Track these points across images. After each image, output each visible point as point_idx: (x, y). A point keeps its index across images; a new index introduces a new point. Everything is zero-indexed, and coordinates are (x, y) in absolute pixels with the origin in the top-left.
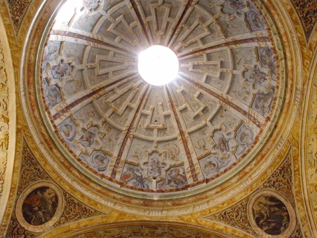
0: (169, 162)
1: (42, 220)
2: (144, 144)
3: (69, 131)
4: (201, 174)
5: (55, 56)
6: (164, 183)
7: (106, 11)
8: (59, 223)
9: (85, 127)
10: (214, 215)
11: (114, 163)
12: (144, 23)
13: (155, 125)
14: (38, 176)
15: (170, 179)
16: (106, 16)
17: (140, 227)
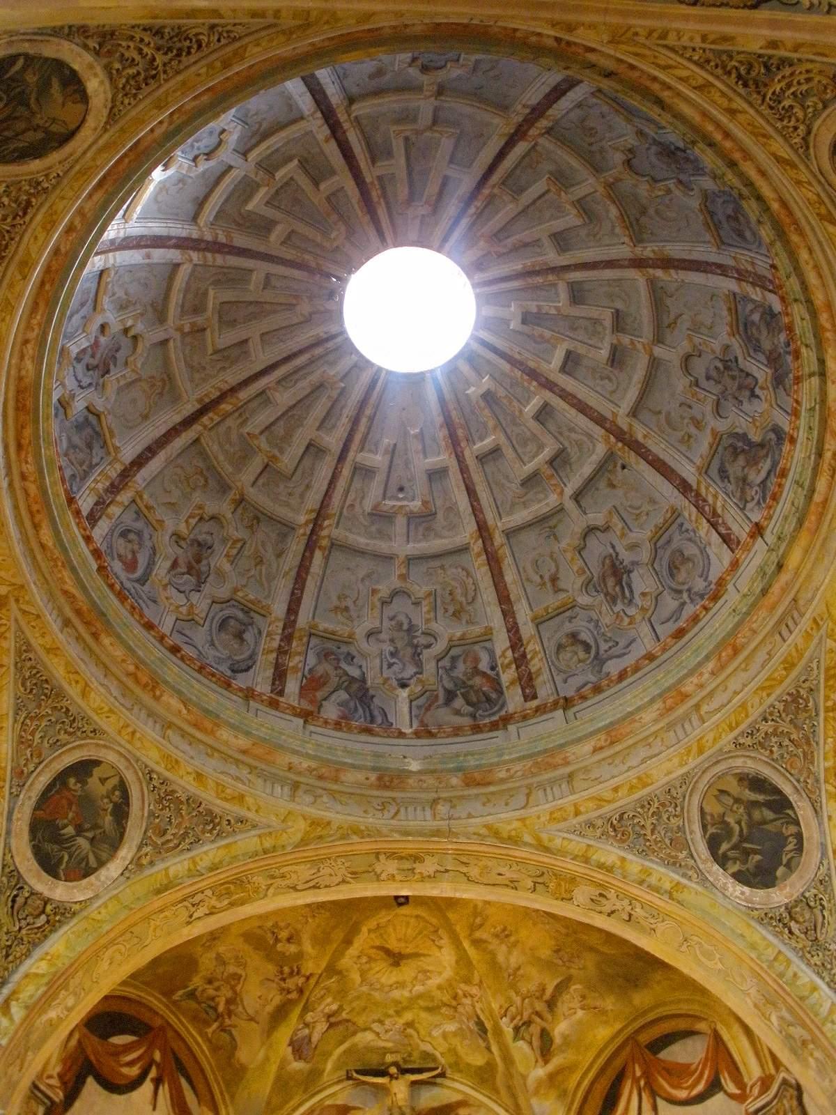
0: (447, 630)
1: (87, 863)
2: (365, 566)
3: (134, 552)
4: (545, 676)
5: (84, 317)
6: (433, 703)
7: (245, 154)
8: (137, 864)
9: (183, 529)
10: (591, 825)
11: (278, 638)
12: (368, 180)
13: (399, 504)
14: (66, 732)
15: (449, 685)
16: (242, 169)
17: (373, 857)
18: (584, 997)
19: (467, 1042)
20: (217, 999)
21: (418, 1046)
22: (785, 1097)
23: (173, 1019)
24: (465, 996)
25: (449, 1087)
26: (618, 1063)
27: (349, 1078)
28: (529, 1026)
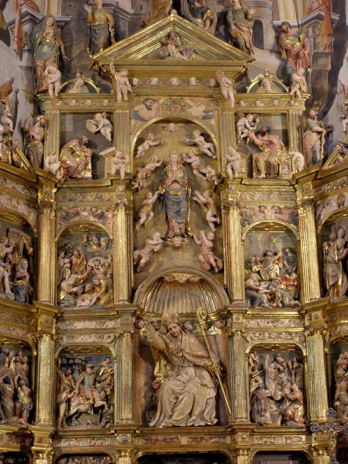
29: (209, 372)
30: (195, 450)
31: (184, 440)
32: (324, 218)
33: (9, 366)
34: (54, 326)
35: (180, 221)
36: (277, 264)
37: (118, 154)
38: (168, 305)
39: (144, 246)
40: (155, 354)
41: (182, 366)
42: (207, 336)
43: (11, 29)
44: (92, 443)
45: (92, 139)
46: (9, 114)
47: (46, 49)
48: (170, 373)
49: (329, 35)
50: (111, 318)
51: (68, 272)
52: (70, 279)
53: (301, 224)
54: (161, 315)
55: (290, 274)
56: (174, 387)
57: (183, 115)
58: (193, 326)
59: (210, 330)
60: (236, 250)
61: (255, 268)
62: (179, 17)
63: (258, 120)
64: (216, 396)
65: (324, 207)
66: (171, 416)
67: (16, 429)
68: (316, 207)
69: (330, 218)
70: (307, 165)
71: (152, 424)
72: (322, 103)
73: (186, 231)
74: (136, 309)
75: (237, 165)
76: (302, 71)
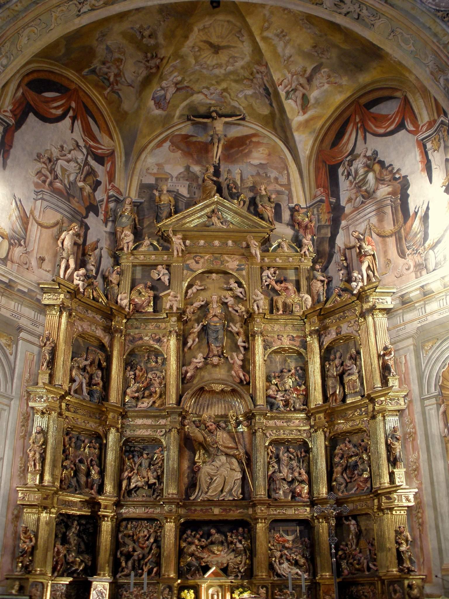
18: (329, 76)
19: (258, 101)
20: (109, 74)
21: (230, 102)
22: (441, 131)
23: (82, 85)
24: (258, 73)
25: (247, 126)
26: (346, 115)
27: (189, 119)
28: (295, 92)
29: (237, 459)
30: (225, 518)
31: (216, 511)
32: (326, 344)
33: (84, 450)
34: (120, 421)
35: (218, 345)
36: (291, 378)
37: (172, 293)
38: (207, 409)
39: (190, 364)
40: (196, 446)
41: (216, 455)
42: (237, 432)
43: (100, 205)
44: (146, 511)
45: (154, 284)
46: (93, 263)
47: (124, 220)
48: (207, 460)
49: (329, 213)
50: (163, 417)
51: (133, 382)
52: (134, 387)
53: (309, 349)
54: (201, 416)
55: (300, 386)
56: (210, 471)
57: (222, 268)
58: (226, 424)
59: (239, 428)
60: (259, 367)
61: (274, 381)
62: (221, 198)
63: (277, 272)
64: (242, 478)
65: (326, 336)
66: (206, 493)
67: (87, 498)
68: (320, 337)
69: (330, 343)
70: (314, 304)
71: (192, 498)
72: (324, 261)
73: (223, 353)
74: (181, 410)
75: (261, 303)
76: (309, 237)
